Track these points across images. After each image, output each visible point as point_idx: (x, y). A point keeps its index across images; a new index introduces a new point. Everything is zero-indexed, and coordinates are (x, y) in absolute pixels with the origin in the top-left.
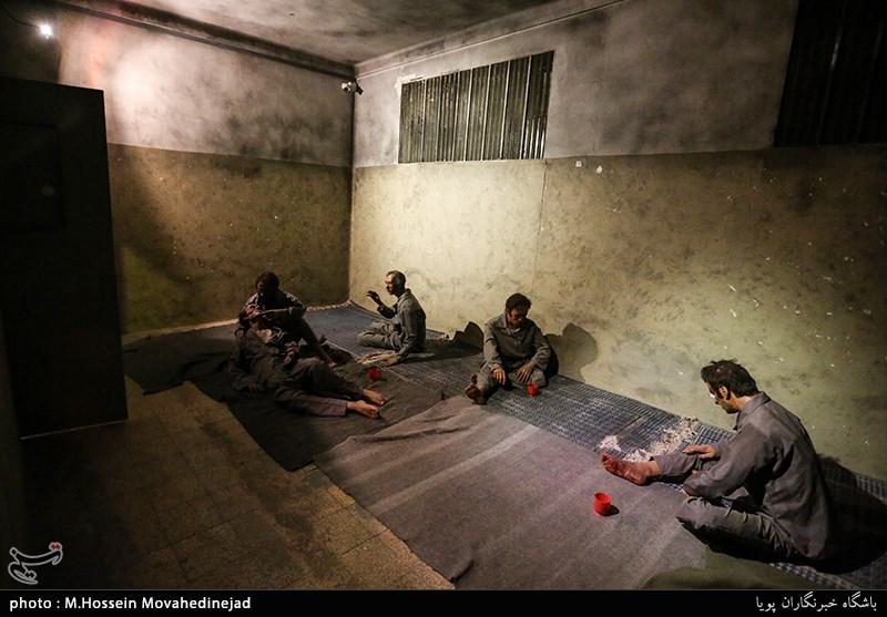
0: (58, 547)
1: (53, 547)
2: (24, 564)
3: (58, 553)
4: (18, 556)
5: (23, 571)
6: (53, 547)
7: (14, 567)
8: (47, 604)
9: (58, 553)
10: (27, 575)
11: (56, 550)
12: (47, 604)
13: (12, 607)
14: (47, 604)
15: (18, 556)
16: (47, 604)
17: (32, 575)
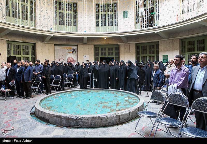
0: (13, 128)
1: (12, 128)
2: (5, 132)
3: (13, 129)
4: (4, 130)
5: (5, 133)
6: (12, 128)
7: (3, 132)
8: (9, 141)
9: (13, 129)
10: (6, 134)
11: (13, 128)
12: (9, 141)
13: (3, 142)
14: (10, 141)
15: (4, 130)
16: (10, 141)
17: (7, 134)
